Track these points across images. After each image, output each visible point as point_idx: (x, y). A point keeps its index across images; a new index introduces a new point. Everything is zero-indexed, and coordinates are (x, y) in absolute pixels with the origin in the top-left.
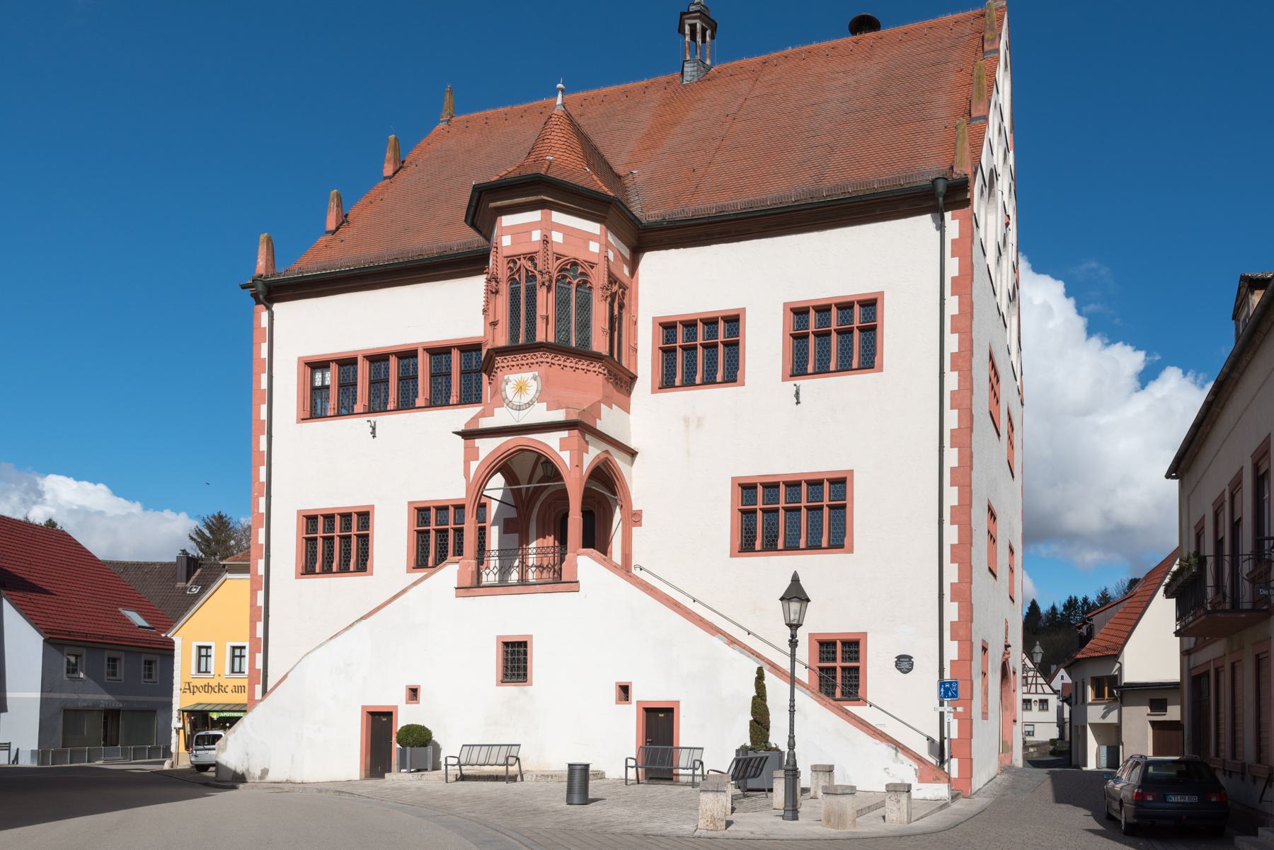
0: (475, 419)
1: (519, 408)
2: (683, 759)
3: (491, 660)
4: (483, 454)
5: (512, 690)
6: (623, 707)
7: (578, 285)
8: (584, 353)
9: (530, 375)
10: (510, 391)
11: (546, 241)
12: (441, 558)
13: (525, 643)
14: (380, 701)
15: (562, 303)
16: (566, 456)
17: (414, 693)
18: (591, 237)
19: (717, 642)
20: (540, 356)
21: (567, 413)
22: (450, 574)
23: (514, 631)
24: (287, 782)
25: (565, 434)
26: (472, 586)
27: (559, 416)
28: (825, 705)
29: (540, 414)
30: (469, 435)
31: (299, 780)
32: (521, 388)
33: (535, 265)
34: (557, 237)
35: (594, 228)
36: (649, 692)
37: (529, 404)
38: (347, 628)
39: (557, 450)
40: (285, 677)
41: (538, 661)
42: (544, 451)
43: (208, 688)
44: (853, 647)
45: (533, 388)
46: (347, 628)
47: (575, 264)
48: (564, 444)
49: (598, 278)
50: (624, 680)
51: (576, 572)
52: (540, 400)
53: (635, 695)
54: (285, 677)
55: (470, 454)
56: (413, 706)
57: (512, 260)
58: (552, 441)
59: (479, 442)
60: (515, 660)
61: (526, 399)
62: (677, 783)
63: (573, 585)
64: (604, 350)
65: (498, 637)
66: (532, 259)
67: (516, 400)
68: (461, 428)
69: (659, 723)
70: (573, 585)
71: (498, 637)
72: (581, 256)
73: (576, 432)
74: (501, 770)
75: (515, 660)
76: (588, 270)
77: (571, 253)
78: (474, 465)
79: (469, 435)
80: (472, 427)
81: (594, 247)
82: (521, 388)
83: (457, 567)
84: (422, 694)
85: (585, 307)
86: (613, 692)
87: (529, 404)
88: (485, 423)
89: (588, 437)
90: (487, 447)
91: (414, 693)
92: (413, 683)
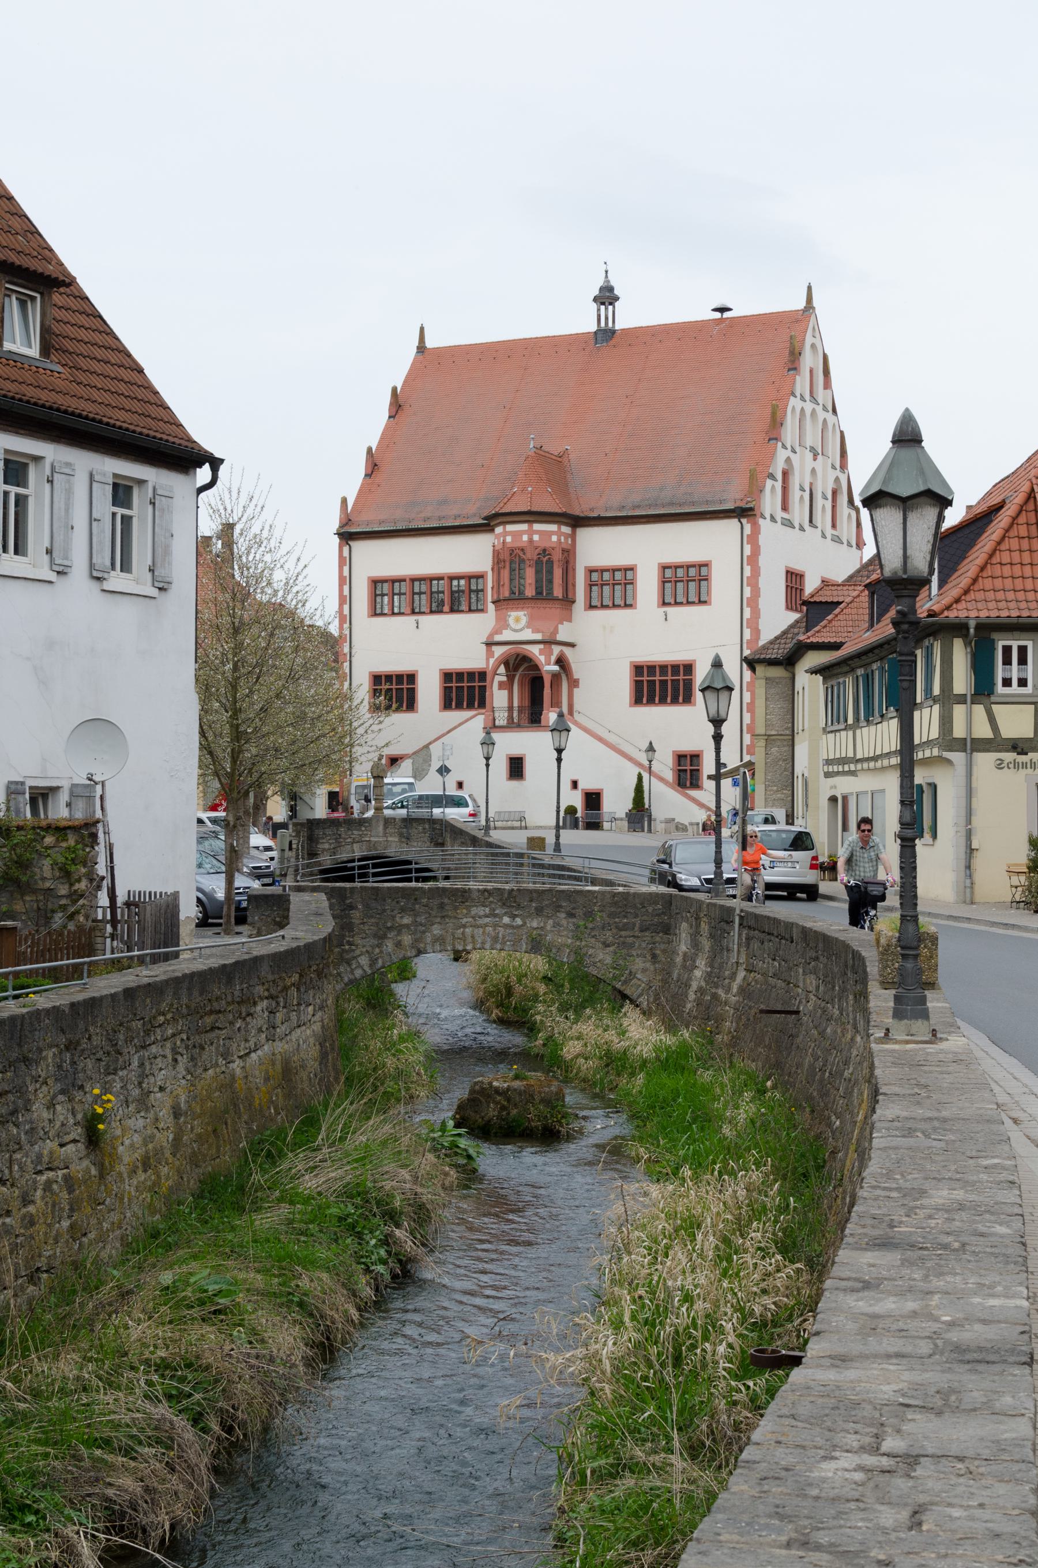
0: (491, 635)
2: (606, 817)
5: (515, 783)
6: (575, 792)
8: (550, 598)
10: (511, 621)
15: (538, 572)
16: (542, 658)
18: (553, 533)
23: (516, 752)
25: (542, 646)
27: (538, 637)
29: (528, 635)
30: (489, 644)
32: (517, 620)
35: (553, 527)
37: (521, 630)
42: (530, 655)
44: (695, 757)
45: (524, 620)
47: (544, 550)
48: (541, 652)
49: (557, 556)
50: (575, 778)
52: (528, 627)
53: (581, 786)
55: (490, 654)
58: (535, 650)
59: (494, 648)
60: (516, 768)
61: (518, 627)
68: (485, 640)
69: (593, 800)
72: (547, 545)
73: (547, 646)
78: (492, 661)
79: (489, 644)
80: (490, 641)
81: (554, 538)
82: (517, 620)
84: (465, 785)
85: (550, 572)
88: (498, 638)
89: (553, 647)
92: (460, 779)
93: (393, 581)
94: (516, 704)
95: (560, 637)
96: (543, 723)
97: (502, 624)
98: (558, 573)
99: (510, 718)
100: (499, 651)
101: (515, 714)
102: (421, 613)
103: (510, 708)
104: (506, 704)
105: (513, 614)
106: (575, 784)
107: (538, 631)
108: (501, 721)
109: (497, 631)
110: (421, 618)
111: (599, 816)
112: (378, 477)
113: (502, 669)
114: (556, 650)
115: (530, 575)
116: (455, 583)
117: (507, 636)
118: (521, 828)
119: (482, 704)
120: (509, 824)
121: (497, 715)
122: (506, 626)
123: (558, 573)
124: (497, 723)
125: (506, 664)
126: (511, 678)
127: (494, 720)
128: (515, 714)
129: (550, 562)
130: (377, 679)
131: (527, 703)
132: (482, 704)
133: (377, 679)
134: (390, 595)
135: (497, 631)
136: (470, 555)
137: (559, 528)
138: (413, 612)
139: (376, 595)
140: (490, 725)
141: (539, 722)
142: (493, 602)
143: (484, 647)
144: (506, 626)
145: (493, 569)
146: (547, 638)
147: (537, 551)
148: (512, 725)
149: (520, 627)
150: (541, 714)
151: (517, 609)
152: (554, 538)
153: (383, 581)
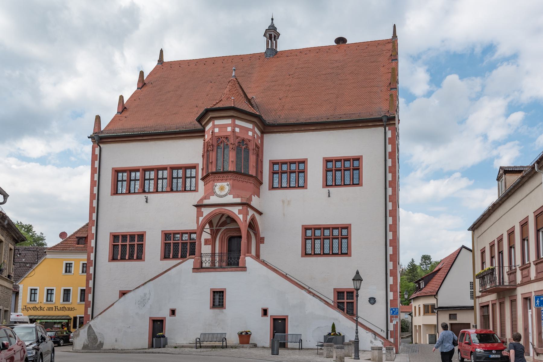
1: (221, 197)
3: (207, 298)
4: (204, 215)
5: (217, 311)
7: (245, 149)
9: (226, 183)
10: (217, 190)
11: (233, 131)
12: (184, 257)
13: (223, 292)
14: (158, 315)
16: (241, 216)
17: (173, 312)
18: (248, 130)
19: (304, 292)
20: (230, 175)
21: (242, 200)
22: (190, 263)
23: (218, 287)
24: (113, 349)
25: (240, 208)
26: (199, 268)
27: (238, 200)
28: (347, 317)
29: (230, 199)
30: (199, 206)
31: (120, 349)
32: (222, 189)
33: (228, 141)
34: (237, 130)
35: (250, 126)
36: (275, 311)
37: (225, 195)
38: (143, 285)
39: (237, 213)
40: (113, 304)
41: (228, 298)
43: (35, 308)
45: (227, 189)
46: (143, 285)
47: (243, 140)
49: (251, 146)
50: (265, 307)
51: (245, 263)
52: (230, 194)
53: (270, 313)
54: (113, 304)
55: (199, 214)
56: (173, 317)
57: (218, 138)
58: (235, 210)
59: (203, 209)
60: (218, 299)
61: (224, 193)
62: (288, 349)
63: (244, 269)
64: (254, 174)
65: (211, 289)
66: (227, 138)
67: (218, 193)
68: (196, 203)
69: (279, 325)
70: (244, 269)
71: (211, 289)
74: (220, 344)
75: (218, 299)
76: (248, 143)
77: (242, 136)
78: (201, 219)
79: (199, 206)
80: (200, 204)
81: (250, 134)
82: (222, 189)
83: (193, 260)
84: (177, 312)
86: (260, 312)
87: (225, 195)
88: (206, 202)
89: (249, 209)
90: (206, 211)
91: (173, 312)
92: (173, 307)
93: (130, 171)
94: (217, 251)
95: (253, 204)
96: (240, 265)
97: (210, 192)
98: (252, 158)
99: (213, 262)
100: (206, 211)
101: (217, 259)
102: (149, 192)
103: (213, 254)
104: (209, 251)
105: (219, 184)
106: (265, 312)
107: (238, 197)
108: (207, 264)
109: (205, 198)
110: (149, 196)
111: (285, 338)
112: (126, 114)
113: (207, 226)
114: (251, 212)
115: (232, 156)
116: (175, 172)
117: (214, 200)
118: (222, 347)
119: (193, 253)
120: (213, 344)
121: (204, 259)
122: (213, 193)
123: (252, 158)
124: (204, 265)
125: (211, 223)
126: (214, 234)
127: (202, 263)
128: (217, 259)
129: (247, 150)
130: (115, 237)
131: (225, 250)
132: (193, 253)
133: (115, 237)
134: (127, 181)
135: (205, 198)
136: (188, 152)
137: (254, 128)
138: (144, 192)
139: (118, 181)
140: (198, 266)
141: (238, 264)
142: (203, 179)
143: (195, 208)
144: (213, 193)
145: (203, 156)
146: (245, 201)
147: (238, 140)
148: (212, 268)
149: (223, 193)
150: (239, 258)
151: (222, 180)
152: (250, 134)
153: (123, 171)
